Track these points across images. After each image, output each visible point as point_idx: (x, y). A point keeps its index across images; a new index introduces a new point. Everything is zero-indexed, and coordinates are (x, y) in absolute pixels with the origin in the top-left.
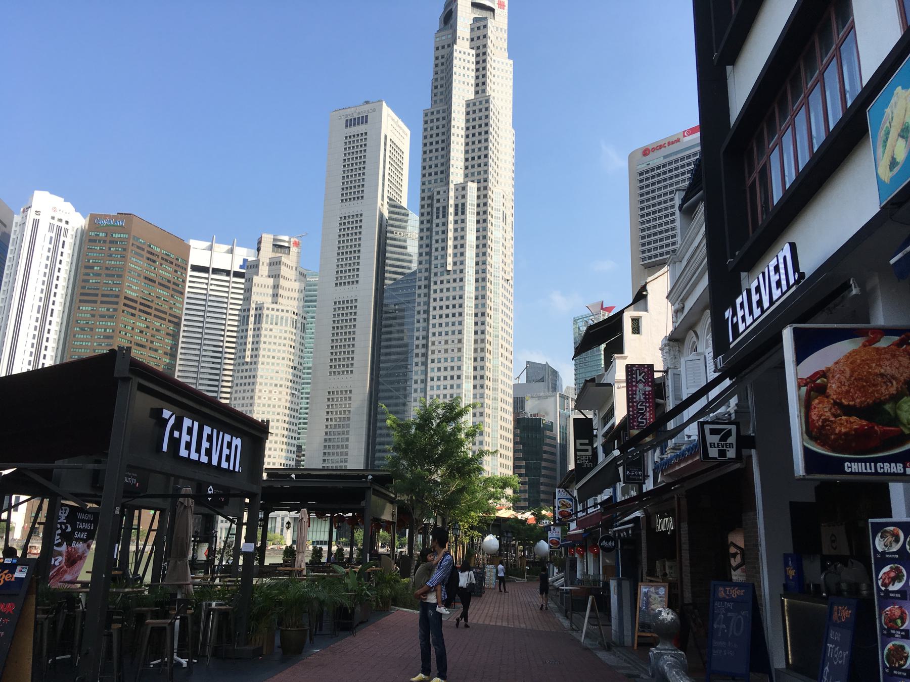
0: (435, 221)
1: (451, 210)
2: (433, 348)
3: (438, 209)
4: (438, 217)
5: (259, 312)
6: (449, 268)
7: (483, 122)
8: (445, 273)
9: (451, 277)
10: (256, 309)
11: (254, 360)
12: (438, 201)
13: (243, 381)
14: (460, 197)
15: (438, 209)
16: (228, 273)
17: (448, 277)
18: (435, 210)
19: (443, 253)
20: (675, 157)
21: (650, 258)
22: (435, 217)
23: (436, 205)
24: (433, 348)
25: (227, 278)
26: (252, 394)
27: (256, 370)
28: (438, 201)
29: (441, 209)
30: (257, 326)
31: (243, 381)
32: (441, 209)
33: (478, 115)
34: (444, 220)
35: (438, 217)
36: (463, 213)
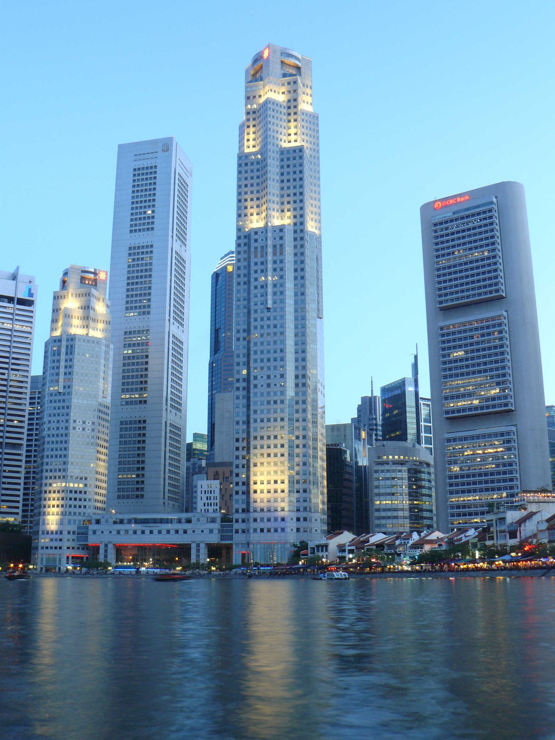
0: (253, 260)
1: (270, 250)
2: (255, 382)
3: (256, 248)
4: (256, 256)
5: (72, 343)
6: (270, 305)
7: (298, 169)
8: (266, 310)
9: (271, 314)
10: (67, 340)
11: (67, 390)
12: (256, 241)
13: (56, 412)
14: (278, 239)
15: (256, 248)
16: (10, 300)
17: (269, 314)
18: (252, 249)
19: (262, 291)
20: (467, 213)
21: (446, 301)
22: (252, 256)
23: (253, 244)
24: (255, 382)
25: (11, 305)
26: (67, 425)
27: (70, 400)
28: (256, 241)
29: (259, 249)
30: (69, 357)
31: (56, 412)
32: (259, 249)
33: (292, 162)
34: (262, 259)
35: (256, 256)
36: (281, 254)
